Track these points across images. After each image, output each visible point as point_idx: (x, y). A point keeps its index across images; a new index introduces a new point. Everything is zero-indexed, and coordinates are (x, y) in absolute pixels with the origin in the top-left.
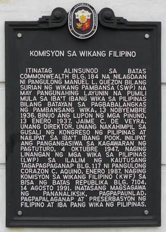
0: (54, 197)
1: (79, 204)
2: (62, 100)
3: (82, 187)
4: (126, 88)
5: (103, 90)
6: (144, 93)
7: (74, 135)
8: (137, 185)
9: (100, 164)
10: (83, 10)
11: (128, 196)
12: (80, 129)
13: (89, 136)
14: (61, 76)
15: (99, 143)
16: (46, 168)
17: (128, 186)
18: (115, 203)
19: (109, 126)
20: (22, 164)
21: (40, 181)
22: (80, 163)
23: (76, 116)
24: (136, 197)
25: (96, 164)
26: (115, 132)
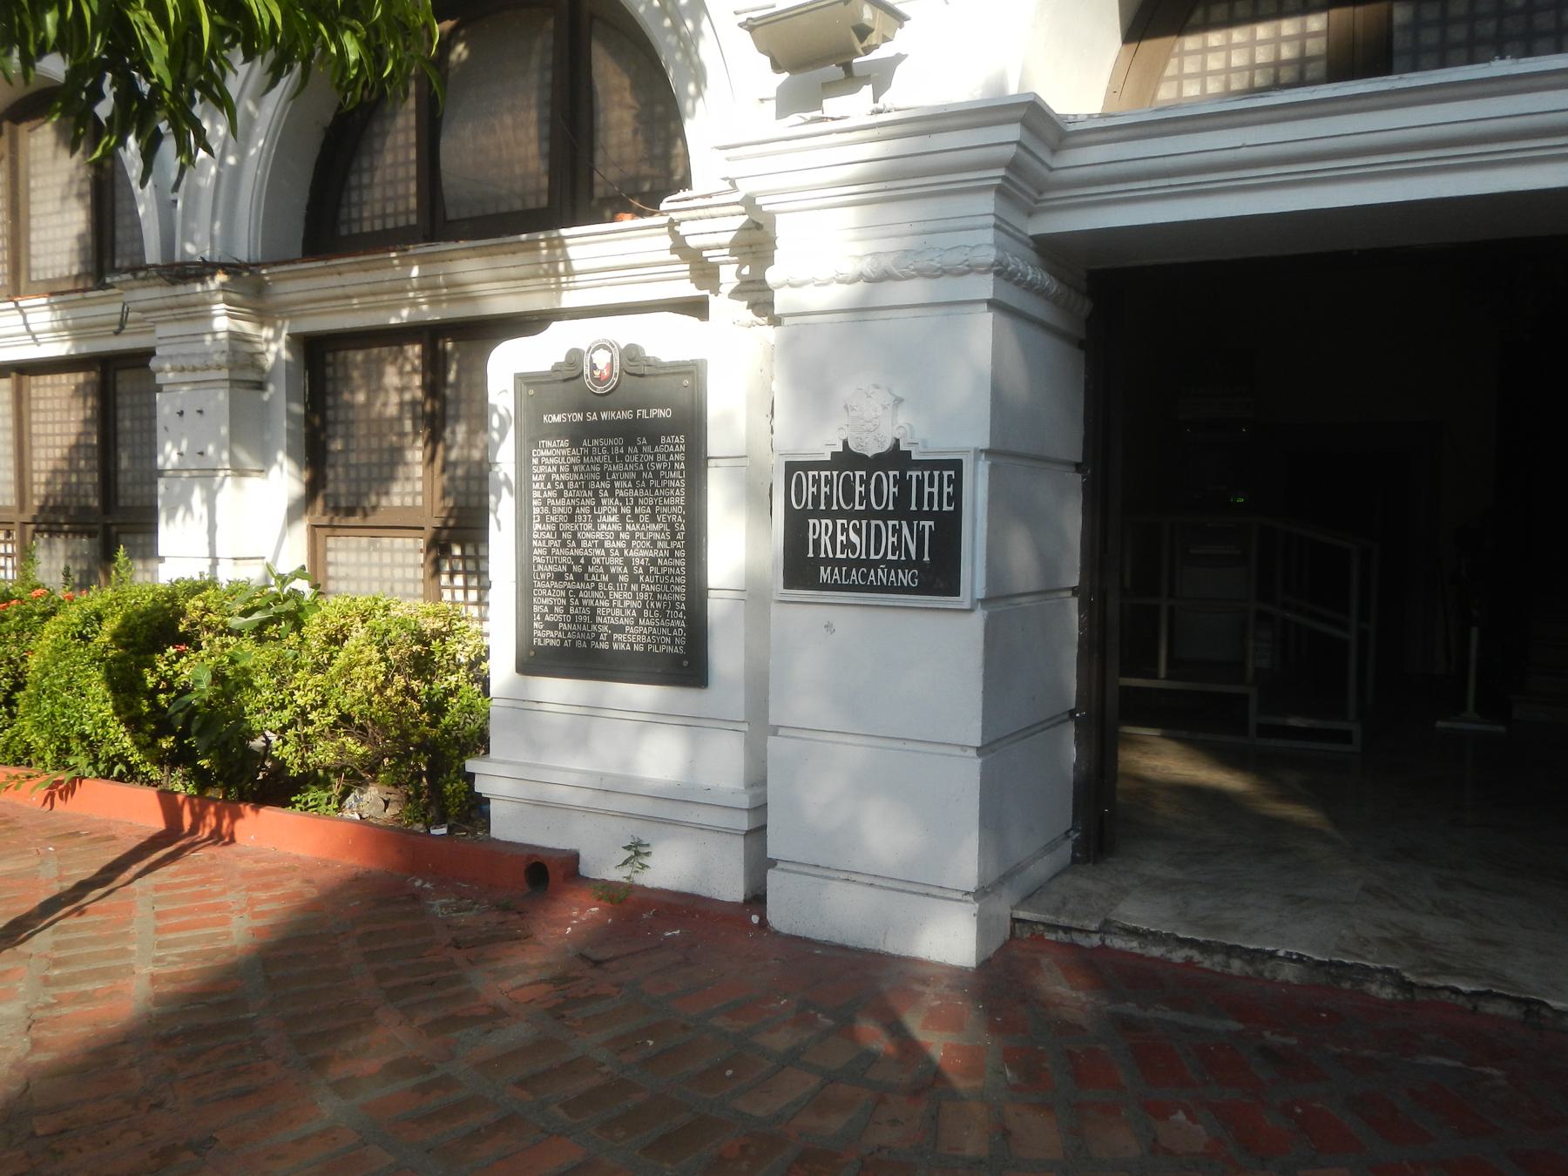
4: (659, 466)
11: (661, 635)
14: (579, 452)
15: (626, 552)
18: (646, 645)
19: (638, 527)
22: (603, 582)
23: (597, 511)
24: (673, 638)
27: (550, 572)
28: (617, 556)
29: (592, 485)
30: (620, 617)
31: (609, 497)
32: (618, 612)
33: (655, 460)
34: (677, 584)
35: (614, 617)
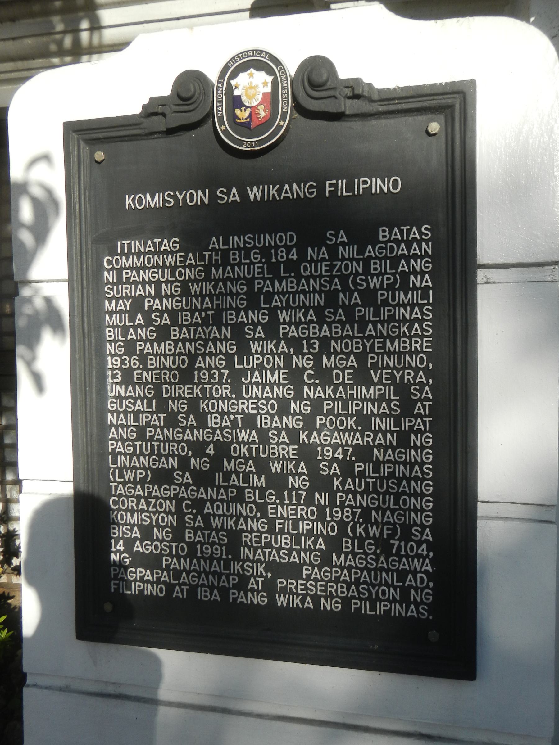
0: (188, 573)
1: (250, 594)
2: (205, 322)
3: (259, 551)
4: (374, 282)
5: (309, 292)
6: (425, 296)
7: (238, 413)
8: (407, 556)
9: (305, 493)
10: (252, 70)
11: (380, 585)
12: (251, 398)
13: (276, 418)
14: (202, 258)
15: (303, 436)
16: (171, 500)
17: (382, 559)
18: (346, 601)
19: (329, 391)
20: (113, 485)
21: (155, 530)
23: (240, 362)
24: (405, 591)
25: (294, 493)
26: (345, 408)
27: (144, 468)
28: (284, 443)
29: (229, 317)
30: (290, 550)
31: (266, 339)
32: (286, 541)
33: (366, 271)
34: (416, 495)
35: (279, 550)
